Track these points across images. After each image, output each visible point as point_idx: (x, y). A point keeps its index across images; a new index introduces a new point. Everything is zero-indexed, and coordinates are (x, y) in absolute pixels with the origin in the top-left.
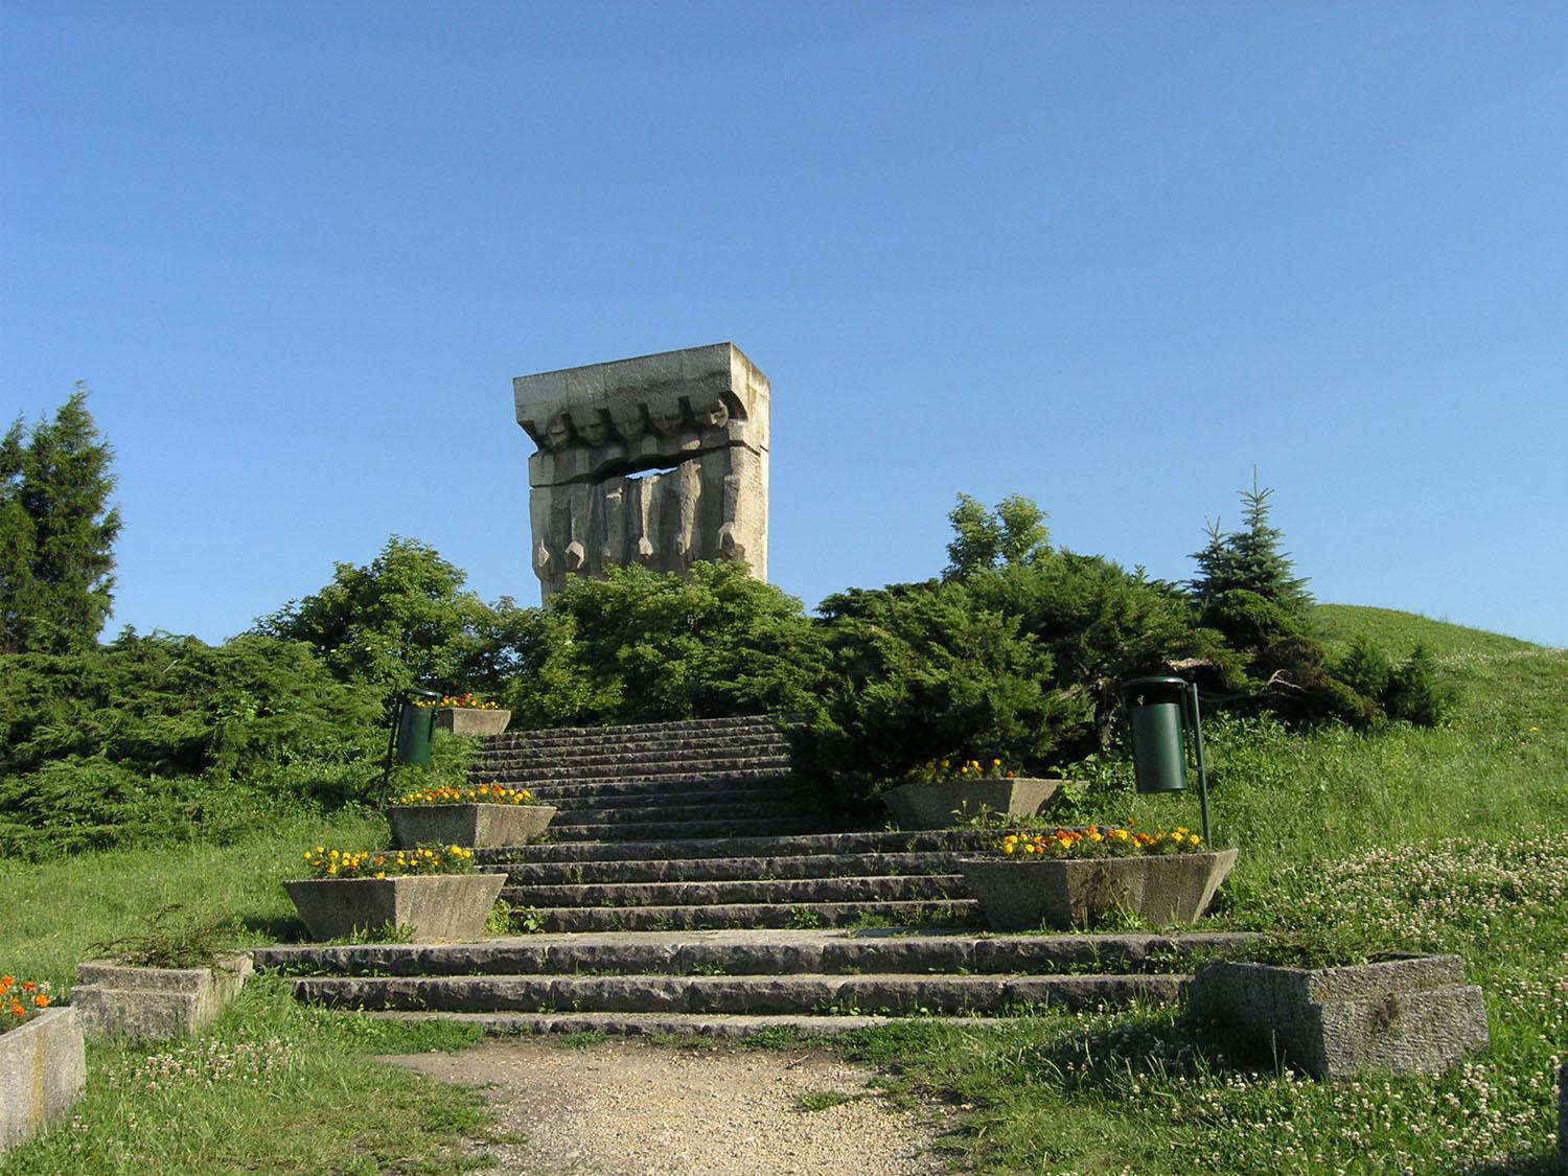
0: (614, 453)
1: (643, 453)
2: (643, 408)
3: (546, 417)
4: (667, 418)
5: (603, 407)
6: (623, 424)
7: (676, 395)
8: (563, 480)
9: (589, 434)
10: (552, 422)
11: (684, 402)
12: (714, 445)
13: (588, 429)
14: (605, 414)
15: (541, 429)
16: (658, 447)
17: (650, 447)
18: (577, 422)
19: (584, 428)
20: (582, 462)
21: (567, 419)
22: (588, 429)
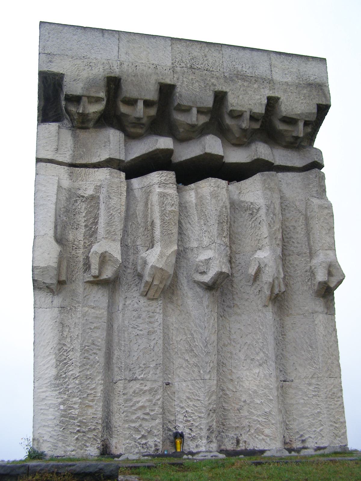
0: (165, 143)
1: (208, 150)
2: (220, 97)
3: (85, 74)
5: (168, 81)
7: (268, 93)
10: (91, 83)
11: (272, 103)
12: (289, 164)
13: (140, 104)
14: (166, 91)
16: (224, 152)
17: (213, 145)
18: (128, 90)
19: (132, 102)
20: (111, 144)
21: (113, 84)
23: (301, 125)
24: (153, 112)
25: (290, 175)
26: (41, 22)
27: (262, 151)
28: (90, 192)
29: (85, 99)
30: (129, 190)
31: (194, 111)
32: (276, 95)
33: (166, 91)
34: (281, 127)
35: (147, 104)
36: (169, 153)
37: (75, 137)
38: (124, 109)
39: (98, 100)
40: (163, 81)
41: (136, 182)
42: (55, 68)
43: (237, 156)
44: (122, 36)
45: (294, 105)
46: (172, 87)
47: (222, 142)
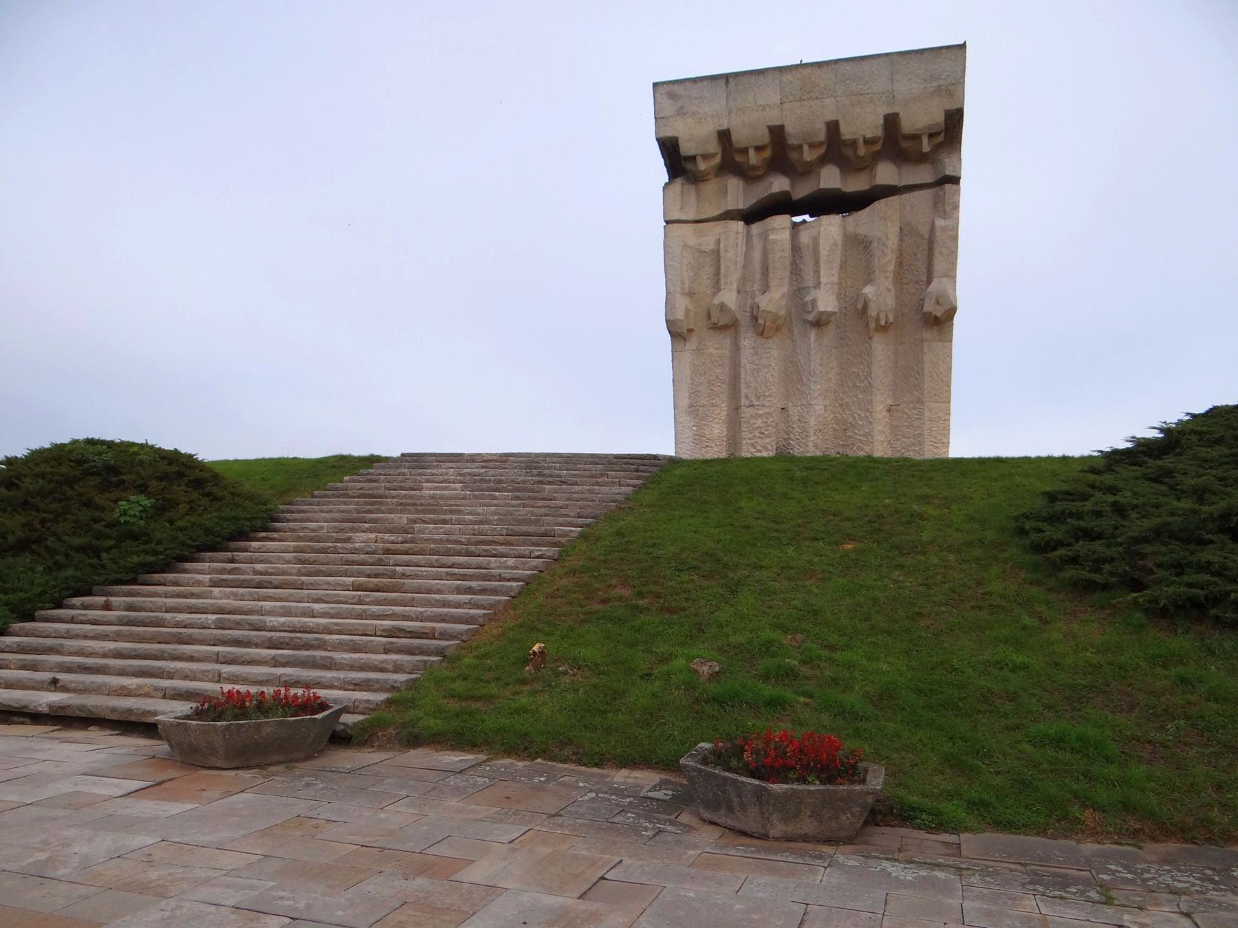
0: (779, 184)
1: (822, 186)
4: (867, 142)
6: (800, 147)
8: (706, 216)
9: (753, 158)
11: (891, 122)
12: (918, 182)
14: (777, 133)
15: (686, 148)
17: (830, 179)
18: (739, 139)
19: (744, 151)
22: (752, 152)
23: (925, 140)
24: (767, 153)
25: (917, 194)
26: (655, 85)
27: (886, 174)
28: (711, 246)
29: (698, 159)
30: (749, 237)
31: (806, 148)
32: (896, 110)
33: (777, 133)
34: (904, 144)
35: (759, 149)
36: (786, 195)
37: (697, 191)
38: (739, 158)
39: (713, 156)
40: (771, 124)
41: (756, 228)
42: (668, 133)
43: (856, 184)
44: (731, 80)
45: (920, 117)
46: (782, 127)
47: (841, 172)
